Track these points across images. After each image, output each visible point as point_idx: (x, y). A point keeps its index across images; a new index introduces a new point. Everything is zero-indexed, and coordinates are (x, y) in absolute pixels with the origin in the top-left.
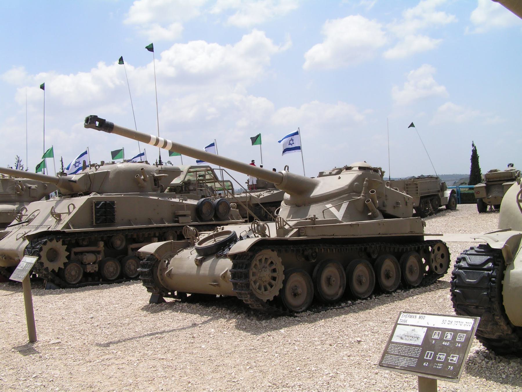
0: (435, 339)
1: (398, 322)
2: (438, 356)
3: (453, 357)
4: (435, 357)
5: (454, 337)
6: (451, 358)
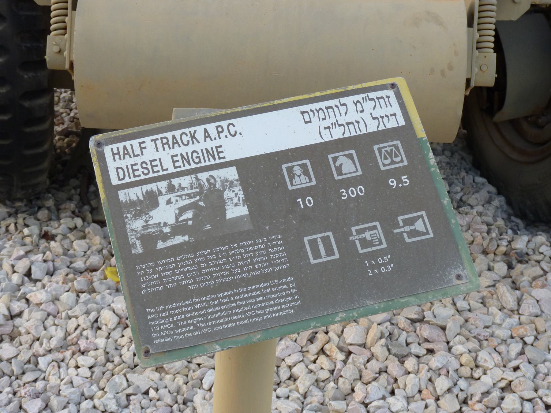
0: (303, 193)
1: (115, 181)
2: (355, 238)
3: (411, 222)
6: (407, 229)
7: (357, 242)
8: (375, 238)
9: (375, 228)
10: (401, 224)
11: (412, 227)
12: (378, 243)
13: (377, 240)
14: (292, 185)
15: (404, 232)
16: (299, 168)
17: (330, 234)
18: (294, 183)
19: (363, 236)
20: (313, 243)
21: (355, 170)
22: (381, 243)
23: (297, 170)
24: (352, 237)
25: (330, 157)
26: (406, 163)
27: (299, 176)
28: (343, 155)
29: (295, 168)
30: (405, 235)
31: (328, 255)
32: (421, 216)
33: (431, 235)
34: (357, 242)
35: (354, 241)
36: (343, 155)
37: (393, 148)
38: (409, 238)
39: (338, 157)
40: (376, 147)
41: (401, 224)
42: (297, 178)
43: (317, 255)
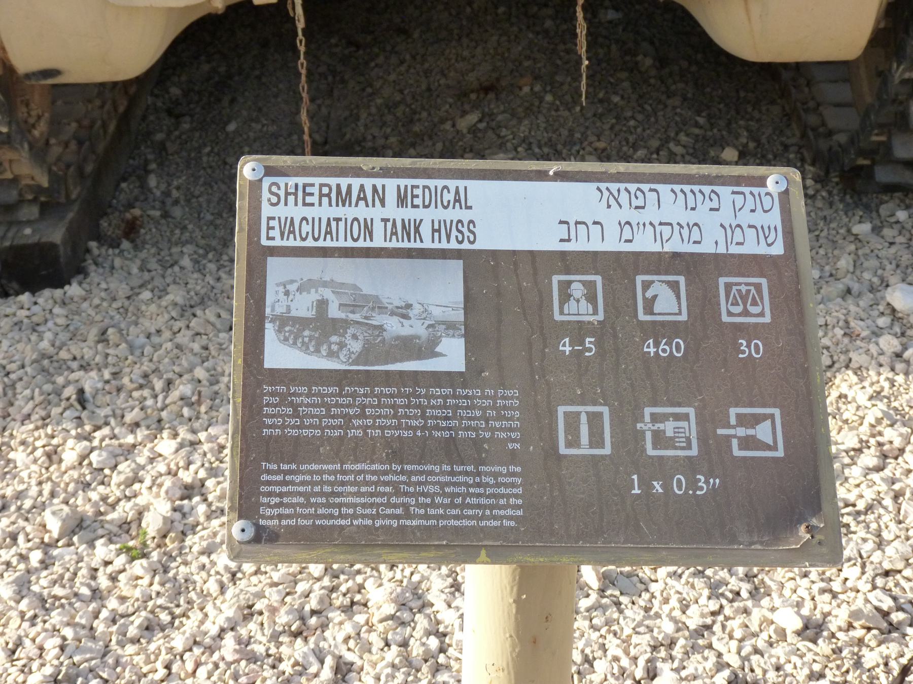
0: (579, 331)
2: (646, 426)
4: (628, 439)
5: (703, 303)
6: (741, 432)
7: (649, 435)
8: (680, 435)
9: (686, 417)
10: (733, 421)
11: (751, 432)
12: (684, 444)
13: (684, 440)
14: (562, 313)
15: (735, 436)
16: (580, 286)
17: (605, 410)
18: (566, 311)
19: (661, 426)
20: (572, 421)
21: (677, 311)
22: (689, 447)
23: (577, 290)
24: (642, 425)
25: (640, 279)
26: (767, 319)
27: (578, 301)
28: (663, 282)
29: (573, 286)
30: (735, 442)
31: (591, 445)
32: (772, 416)
33: (780, 453)
34: (649, 435)
35: (643, 432)
36: (663, 282)
37: (752, 288)
38: (741, 448)
39: (653, 282)
40: (722, 281)
41: (733, 421)
42: (572, 302)
43: (573, 442)
